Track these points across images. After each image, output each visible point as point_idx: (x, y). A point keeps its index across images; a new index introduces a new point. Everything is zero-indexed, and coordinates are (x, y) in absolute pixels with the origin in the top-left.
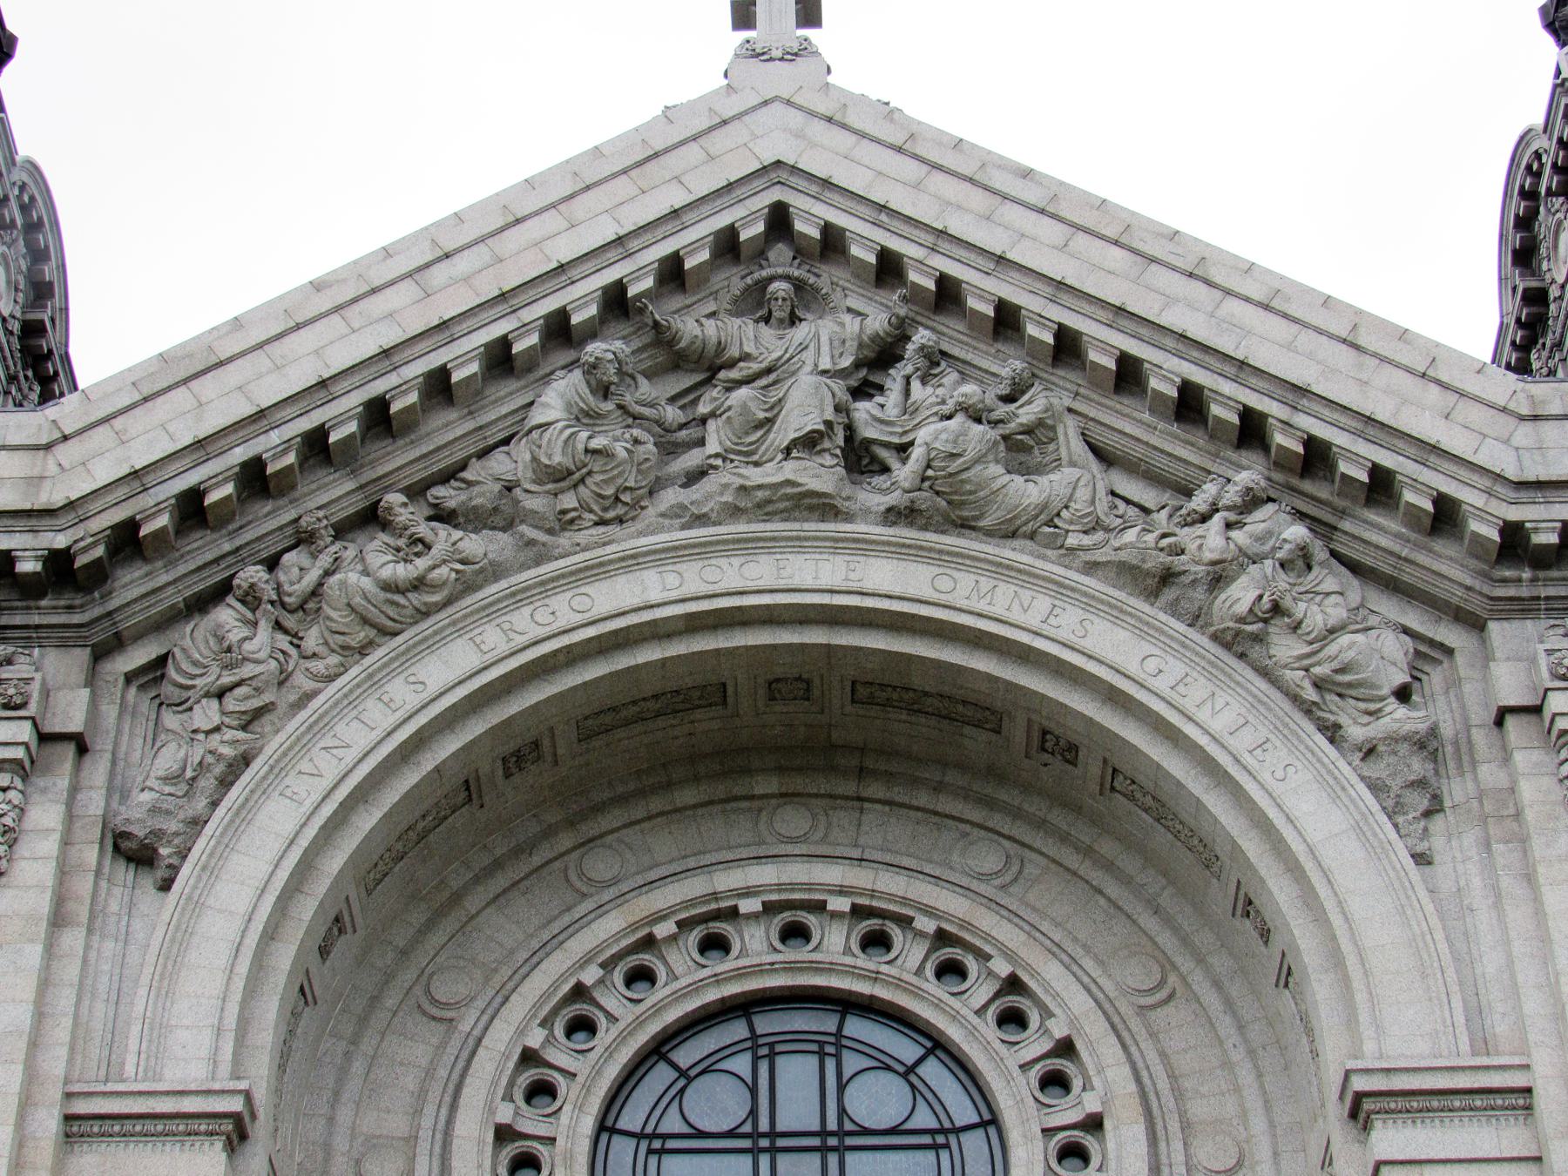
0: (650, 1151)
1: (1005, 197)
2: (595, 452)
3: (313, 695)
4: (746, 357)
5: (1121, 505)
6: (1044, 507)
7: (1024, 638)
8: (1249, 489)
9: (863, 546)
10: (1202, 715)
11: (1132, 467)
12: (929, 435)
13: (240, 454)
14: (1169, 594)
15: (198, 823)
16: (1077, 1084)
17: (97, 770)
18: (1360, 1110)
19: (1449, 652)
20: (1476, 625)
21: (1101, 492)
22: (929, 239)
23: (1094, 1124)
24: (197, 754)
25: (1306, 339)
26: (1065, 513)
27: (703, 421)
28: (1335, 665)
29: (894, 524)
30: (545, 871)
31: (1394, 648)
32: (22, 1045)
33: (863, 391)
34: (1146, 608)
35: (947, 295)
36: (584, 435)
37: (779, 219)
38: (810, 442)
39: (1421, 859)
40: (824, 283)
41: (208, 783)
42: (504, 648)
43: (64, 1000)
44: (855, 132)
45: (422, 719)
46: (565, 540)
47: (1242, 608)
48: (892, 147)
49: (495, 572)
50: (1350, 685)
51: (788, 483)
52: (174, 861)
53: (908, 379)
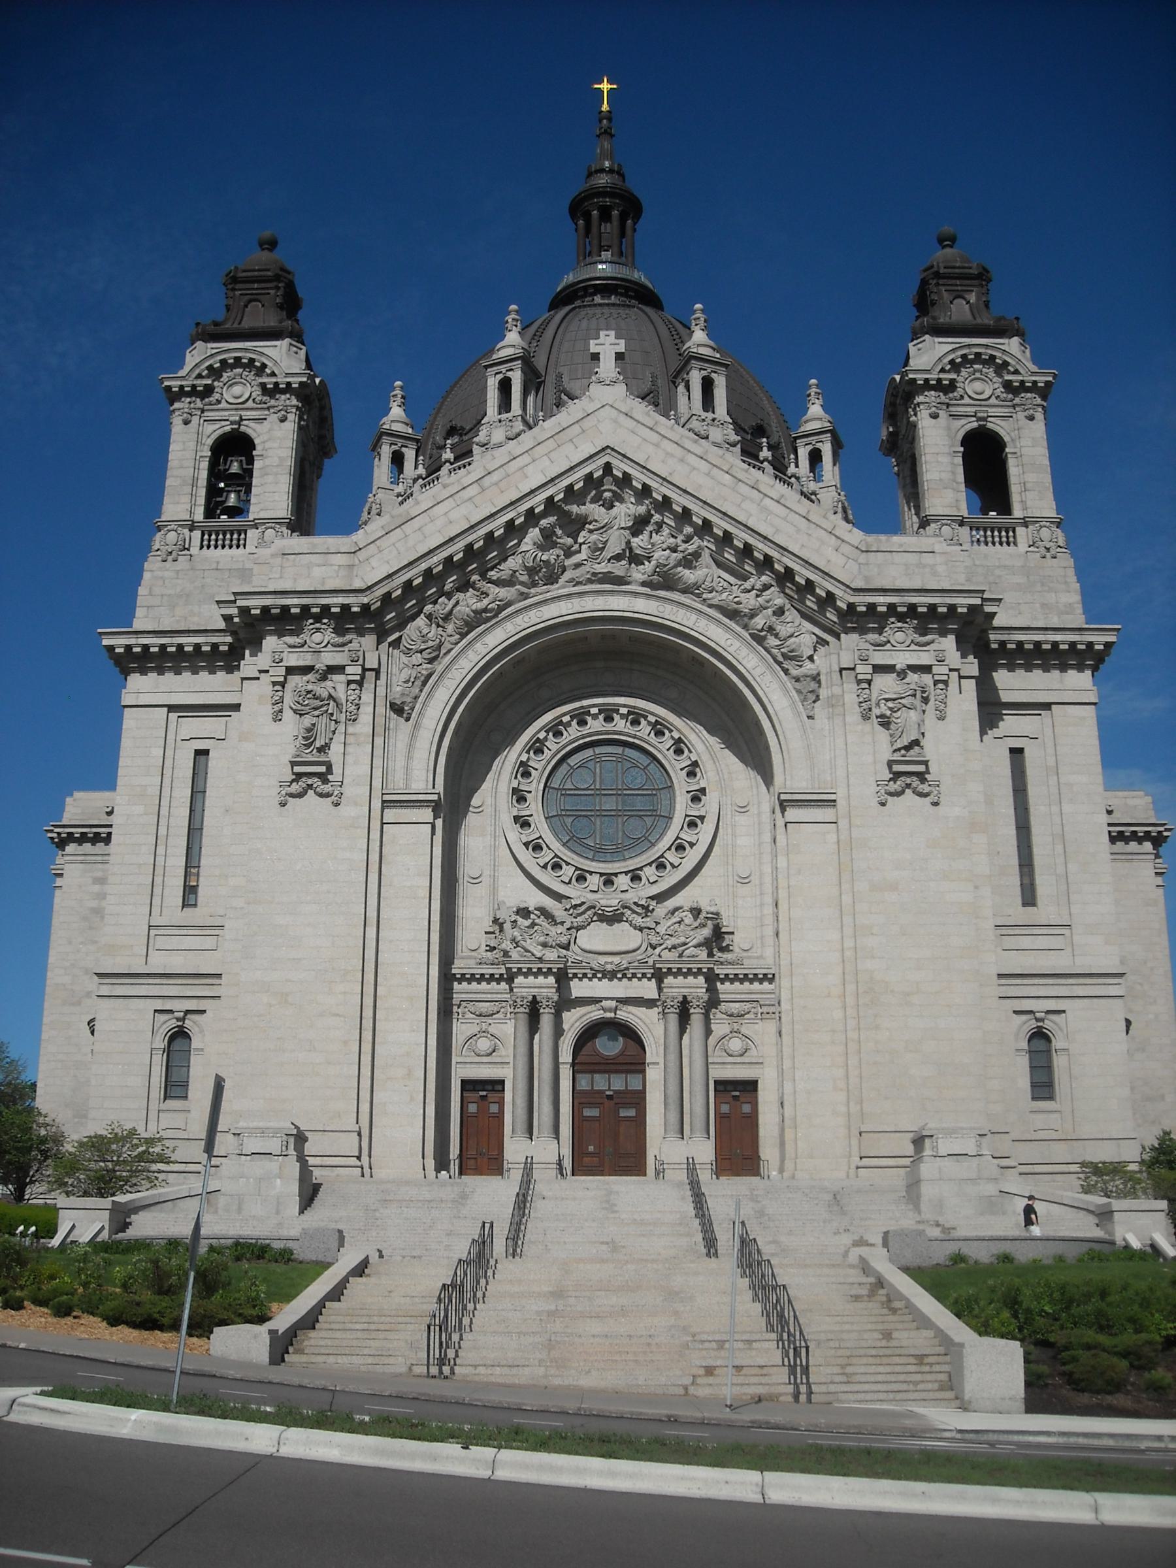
0: (562, 795)
1: (689, 451)
3: (452, 649)
7: (687, 630)
12: (659, 555)
13: (424, 566)
15: (416, 698)
16: (699, 775)
17: (382, 682)
18: (783, 805)
19: (828, 643)
20: (838, 637)
22: (660, 481)
27: (581, 545)
28: (789, 649)
35: (666, 502)
36: (540, 554)
37: (608, 467)
38: (618, 558)
41: (418, 683)
44: (636, 420)
45: (487, 658)
47: (760, 627)
49: (509, 604)
51: (609, 572)
53: (651, 532)
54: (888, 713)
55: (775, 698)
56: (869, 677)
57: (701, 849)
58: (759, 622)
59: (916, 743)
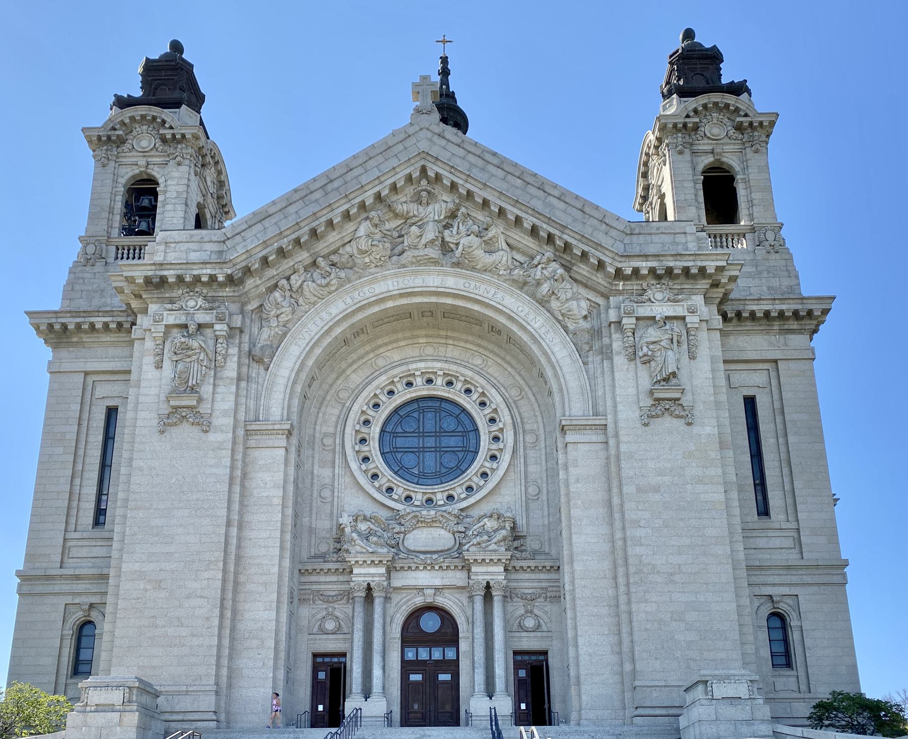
4: (415, 216)
5: (515, 262)
6: (494, 262)
9: (446, 274)
10: (532, 323)
11: (518, 250)
14: (526, 288)
19: (599, 305)
21: (509, 258)
23: (501, 430)
24: (273, 333)
25: (570, 209)
27: (403, 236)
31: (584, 304)
32: (233, 412)
33: (447, 226)
34: (519, 292)
39: (585, 363)
42: (352, 303)
43: (242, 400)
47: (544, 293)
48: (457, 145)
50: (571, 315)
51: (426, 255)
52: (268, 363)
54: (650, 353)
55: (557, 349)
56: (633, 326)
58: (545, 288)
59: (674, 374)
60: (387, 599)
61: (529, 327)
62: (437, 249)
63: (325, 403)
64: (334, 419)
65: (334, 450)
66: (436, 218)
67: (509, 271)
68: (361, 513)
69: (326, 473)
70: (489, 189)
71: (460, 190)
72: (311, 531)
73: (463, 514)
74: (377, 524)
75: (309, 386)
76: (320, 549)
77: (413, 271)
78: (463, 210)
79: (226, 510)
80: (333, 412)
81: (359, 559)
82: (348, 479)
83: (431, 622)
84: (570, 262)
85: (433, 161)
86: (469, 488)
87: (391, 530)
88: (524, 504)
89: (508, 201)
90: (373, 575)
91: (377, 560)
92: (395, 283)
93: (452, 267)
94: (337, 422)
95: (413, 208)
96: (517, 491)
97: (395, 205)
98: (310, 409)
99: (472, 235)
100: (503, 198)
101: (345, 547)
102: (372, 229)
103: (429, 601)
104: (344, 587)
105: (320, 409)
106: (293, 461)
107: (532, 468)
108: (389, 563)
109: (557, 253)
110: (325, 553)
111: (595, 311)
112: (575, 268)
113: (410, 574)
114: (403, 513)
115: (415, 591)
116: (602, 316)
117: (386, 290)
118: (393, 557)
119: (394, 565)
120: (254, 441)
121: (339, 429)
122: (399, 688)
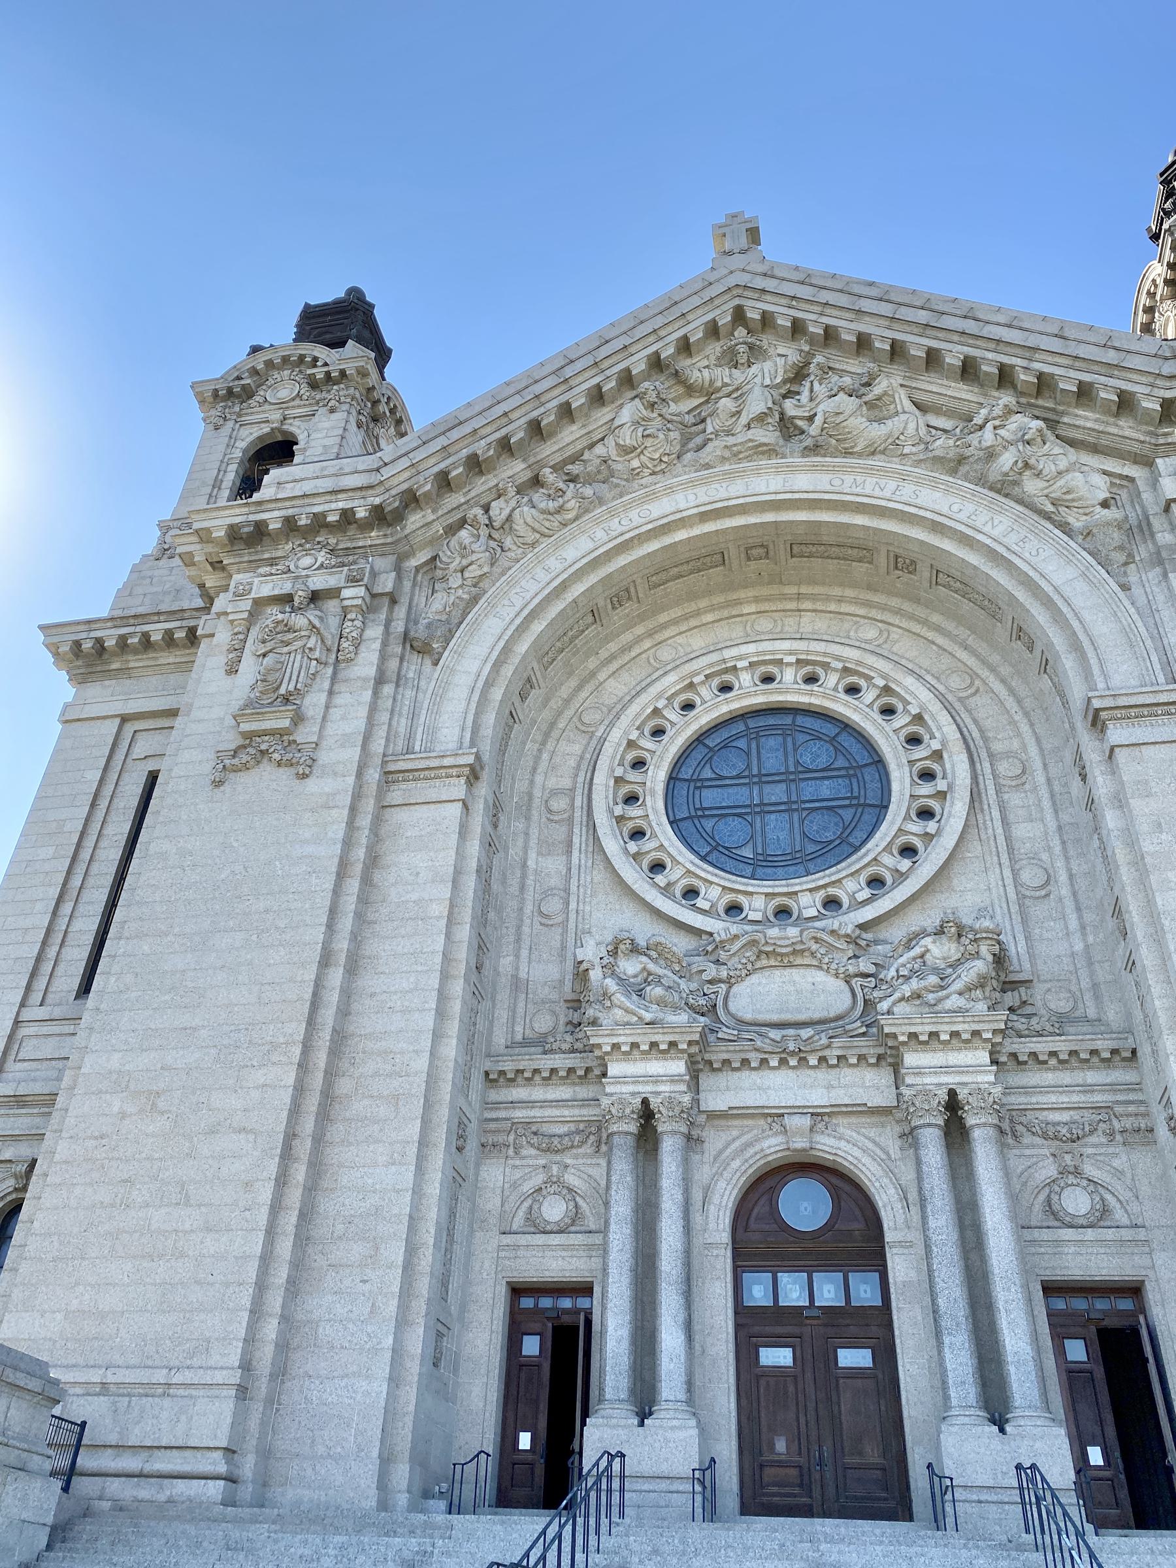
0: (696, 788)
2: (648, 436)
8: (1006, 406)
9: (793, 469)
14: (964, 469)
19: (1132, 480)
26: (902, 437)
27: (703, 421)
29: (808, 456)
30: (637, 660)
34: (951, 479)
37: (739, 315)
40: (765, 344)
42: (606, 538)
46: (635, 485)
47: (1006, 468)
50: (1073, 500)
51: (751, 440)
57: (948, 841)
58: (1007, 460)
60: (692, 1141)
61: (979, 537)
62: (771, 429)
63: (555, 734)
64: (572, 763)
65: (571, 820)
66: (767, 382)
67: (922, 446)
68: (626, 935)
69: (554, 865)
70: (867, 319)
71: (811, 329)
72: (518, 985)
73: (864, 936)
74: (662, 962)
75: (523, 697)
76: (536, 1026)
77: (725, 473)
78: (819, 359)
79: (323, 929)
80: (571, 749)
81: (621, 1039)
82: (600, 875)
83: (805, 1204)
84: (1053, 410)
85: (756, 296)
86: (876, 882)
87: (696, 978)
88: (1014, 908)
89: (908, 329)
90: (656, 1079)
91: (663, 1040)
92: (691, 497)
93: (803, 456)
94: (578, 768)
95: (723, 375)
96: (994, 877)
97: (687, 372)
98: (524, 743)
99: (841, 394)
100: (895, 326)
101: (590, 1013)
102: (644, 412)
103: (799, 1146)
104: (588, 1113)
105: (544, 743)
106: (479, 830)
107: (1021, 831)
108: (694, 1049)
109: (1023, 400)
110: (546, 1035)
111: (1124, 494)
112: (1066, 420)
113: (747, 1078)
114: (723, 937)
115: (762, 1122)
116: (1144, 496)
117: (673, 509)
118: (703, 1035)
119: (707, 1057)
120: (398, 793)
121: (580, 779)
122: (733, 1388)
